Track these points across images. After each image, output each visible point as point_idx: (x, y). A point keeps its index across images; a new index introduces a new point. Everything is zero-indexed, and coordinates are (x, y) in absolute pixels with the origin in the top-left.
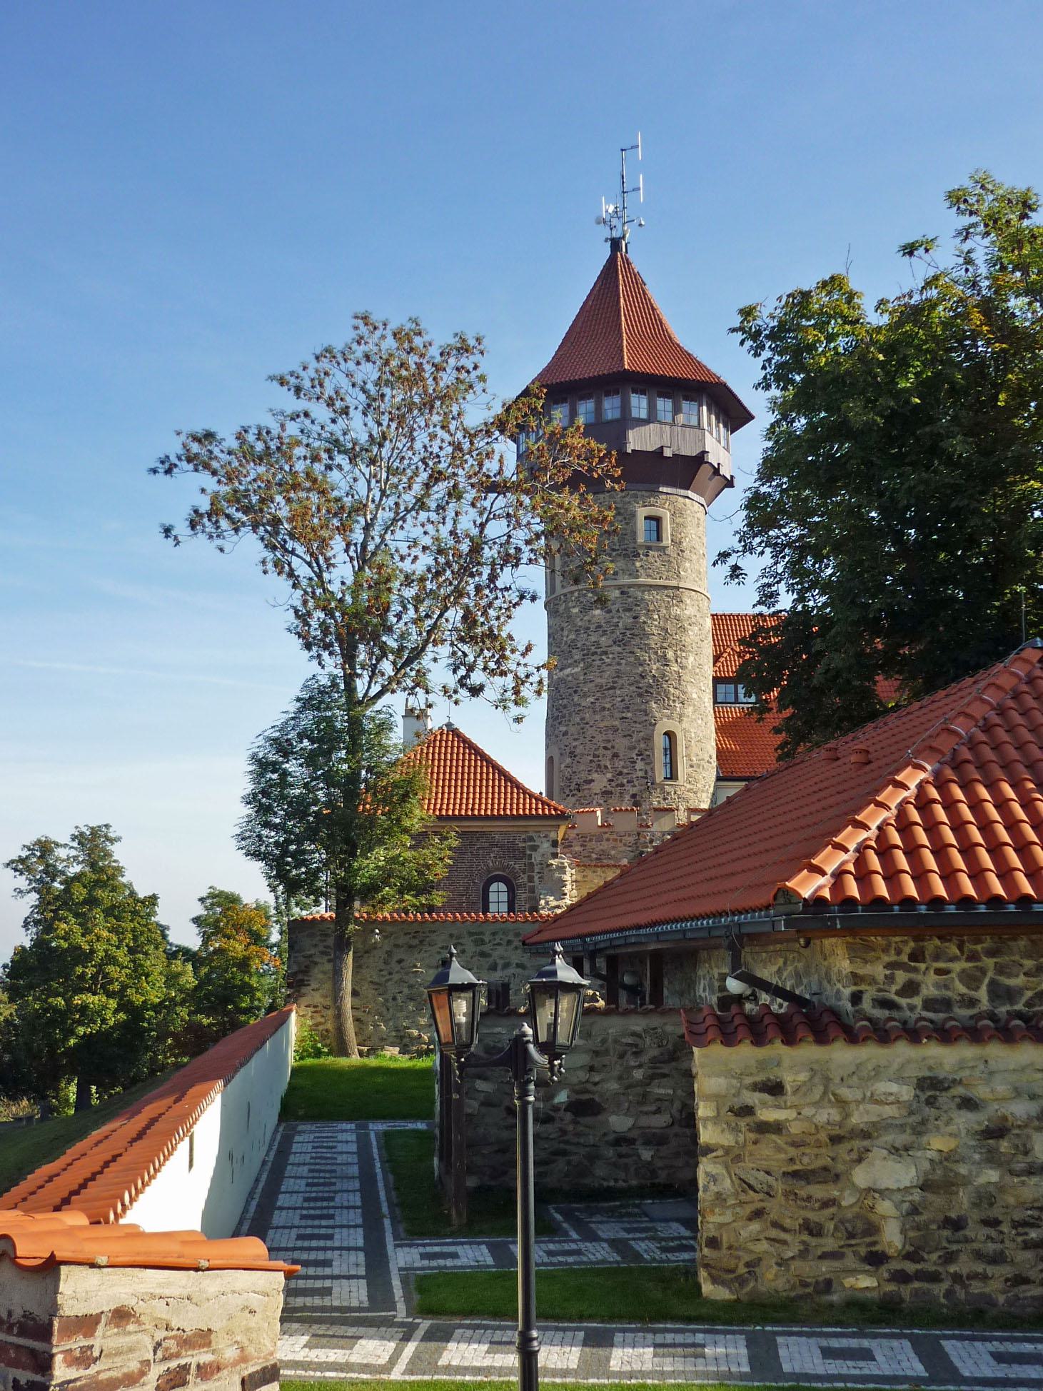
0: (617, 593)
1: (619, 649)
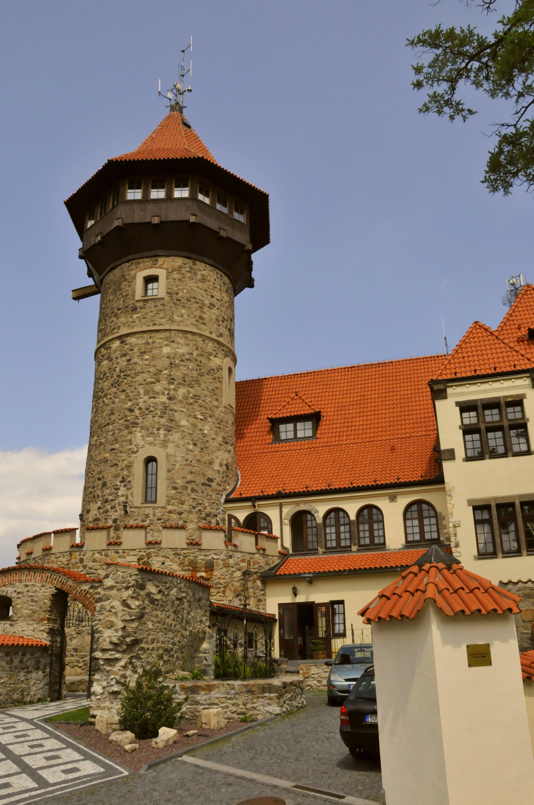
0: (117, 344)
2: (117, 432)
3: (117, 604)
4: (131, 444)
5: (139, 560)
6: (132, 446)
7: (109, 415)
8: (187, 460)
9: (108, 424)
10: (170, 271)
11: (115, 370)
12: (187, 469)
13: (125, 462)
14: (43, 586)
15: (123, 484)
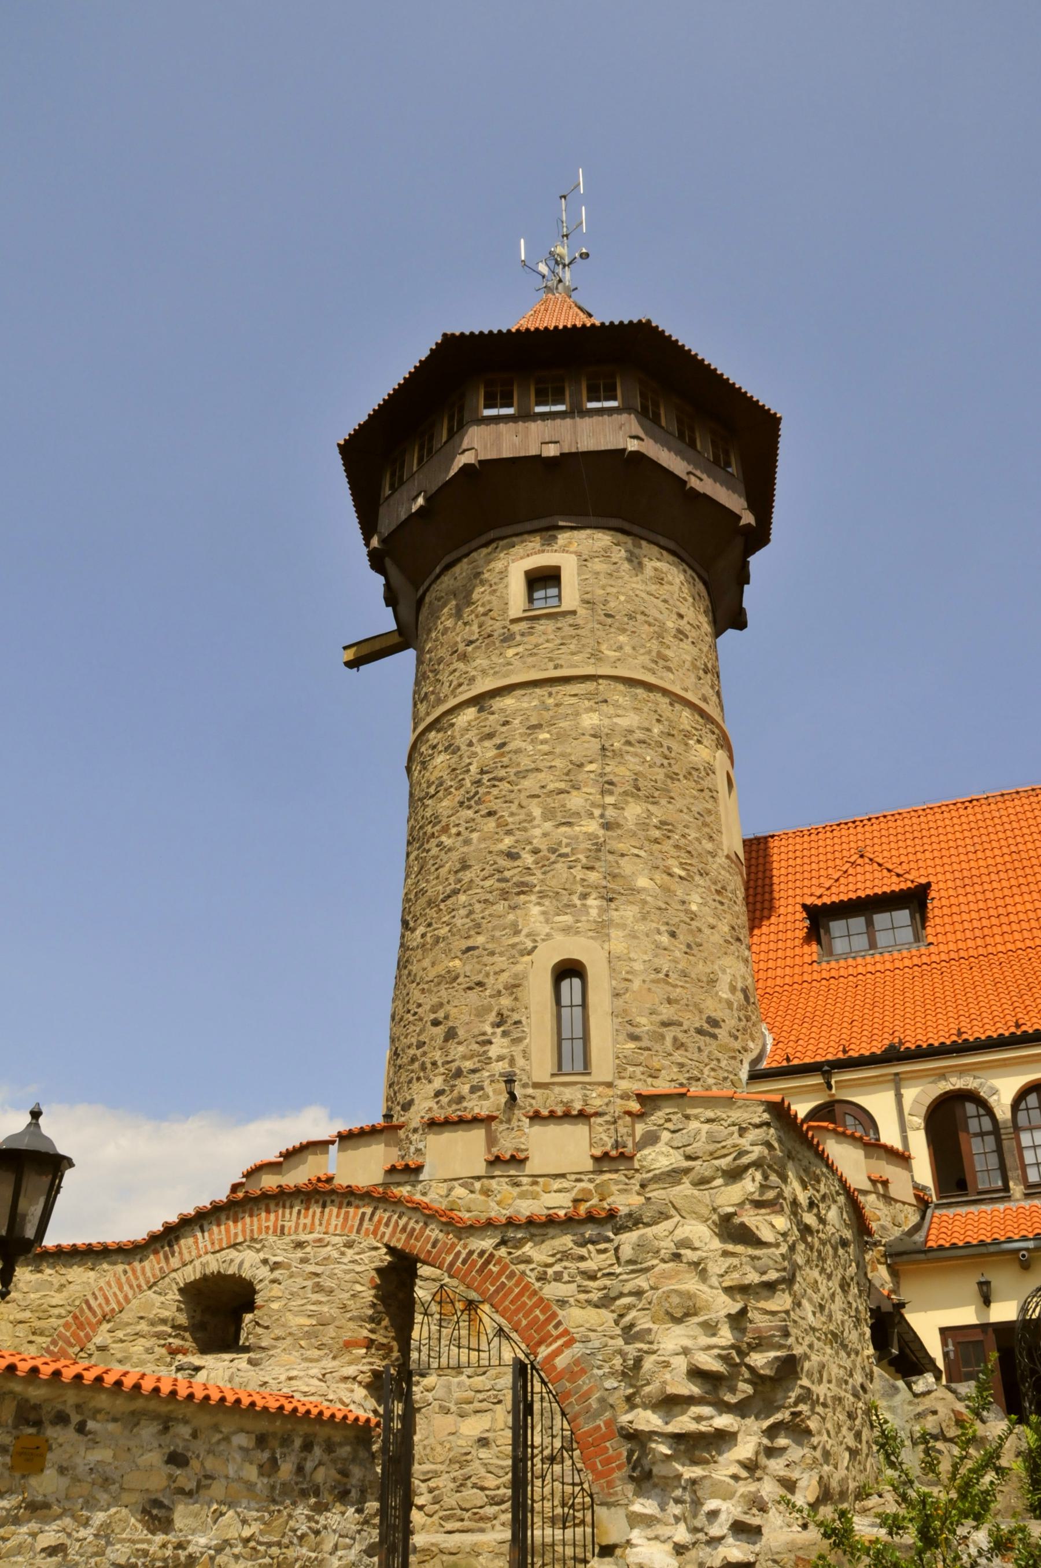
1: (470, 813)
2: (478, 907)
3: (700, 1233)
4: (517, 933)
5: (576, 1201)
6: (521, 938)
7: (456, 872)
8: (657, 971)
9: (456, 892)
10: (585, 557)
11: (468, 771)
12: (661, 991)
13: (504, 977)
14: (349, 1245)
15: (499, 1031)
